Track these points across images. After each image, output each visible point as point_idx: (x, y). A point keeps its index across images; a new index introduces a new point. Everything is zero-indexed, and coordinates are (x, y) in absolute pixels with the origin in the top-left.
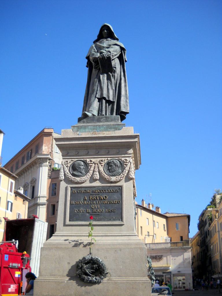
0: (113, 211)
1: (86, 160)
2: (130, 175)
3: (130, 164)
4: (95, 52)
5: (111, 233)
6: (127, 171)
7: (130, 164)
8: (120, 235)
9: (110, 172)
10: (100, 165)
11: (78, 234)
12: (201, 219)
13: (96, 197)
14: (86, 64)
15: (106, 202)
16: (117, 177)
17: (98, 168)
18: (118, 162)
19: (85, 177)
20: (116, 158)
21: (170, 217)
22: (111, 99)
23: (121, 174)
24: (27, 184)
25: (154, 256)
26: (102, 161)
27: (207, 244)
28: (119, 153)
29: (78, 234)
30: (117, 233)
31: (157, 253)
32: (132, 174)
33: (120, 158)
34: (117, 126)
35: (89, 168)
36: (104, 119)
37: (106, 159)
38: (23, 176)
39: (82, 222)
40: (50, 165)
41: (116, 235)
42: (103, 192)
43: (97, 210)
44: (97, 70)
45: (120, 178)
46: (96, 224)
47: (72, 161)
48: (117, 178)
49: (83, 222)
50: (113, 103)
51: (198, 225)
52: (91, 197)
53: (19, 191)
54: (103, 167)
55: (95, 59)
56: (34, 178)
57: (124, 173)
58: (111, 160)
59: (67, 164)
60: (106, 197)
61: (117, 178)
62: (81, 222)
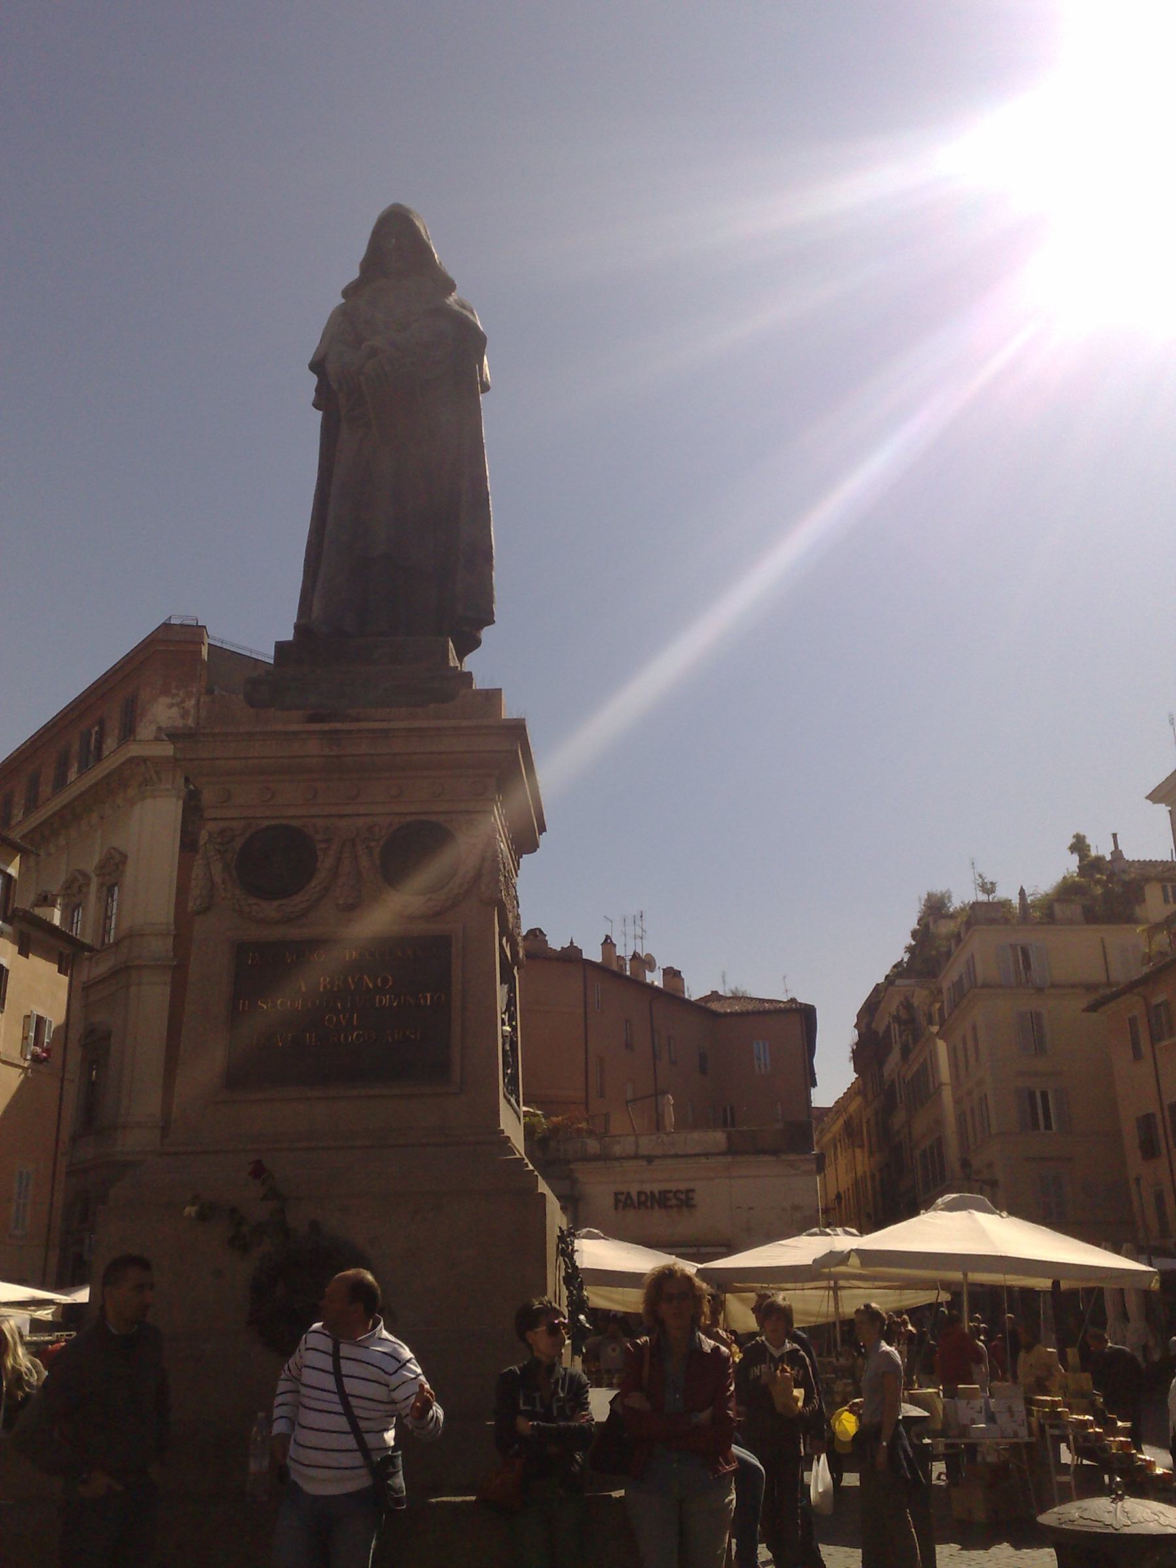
0: (413, 1037)
12: (868, 1025)
24: (80, 877)
38: (62, 841)
40: (190, 791)
43: (346, 1037)
51: (853, 1051)
53: (40, 912)
56: (114, 849)
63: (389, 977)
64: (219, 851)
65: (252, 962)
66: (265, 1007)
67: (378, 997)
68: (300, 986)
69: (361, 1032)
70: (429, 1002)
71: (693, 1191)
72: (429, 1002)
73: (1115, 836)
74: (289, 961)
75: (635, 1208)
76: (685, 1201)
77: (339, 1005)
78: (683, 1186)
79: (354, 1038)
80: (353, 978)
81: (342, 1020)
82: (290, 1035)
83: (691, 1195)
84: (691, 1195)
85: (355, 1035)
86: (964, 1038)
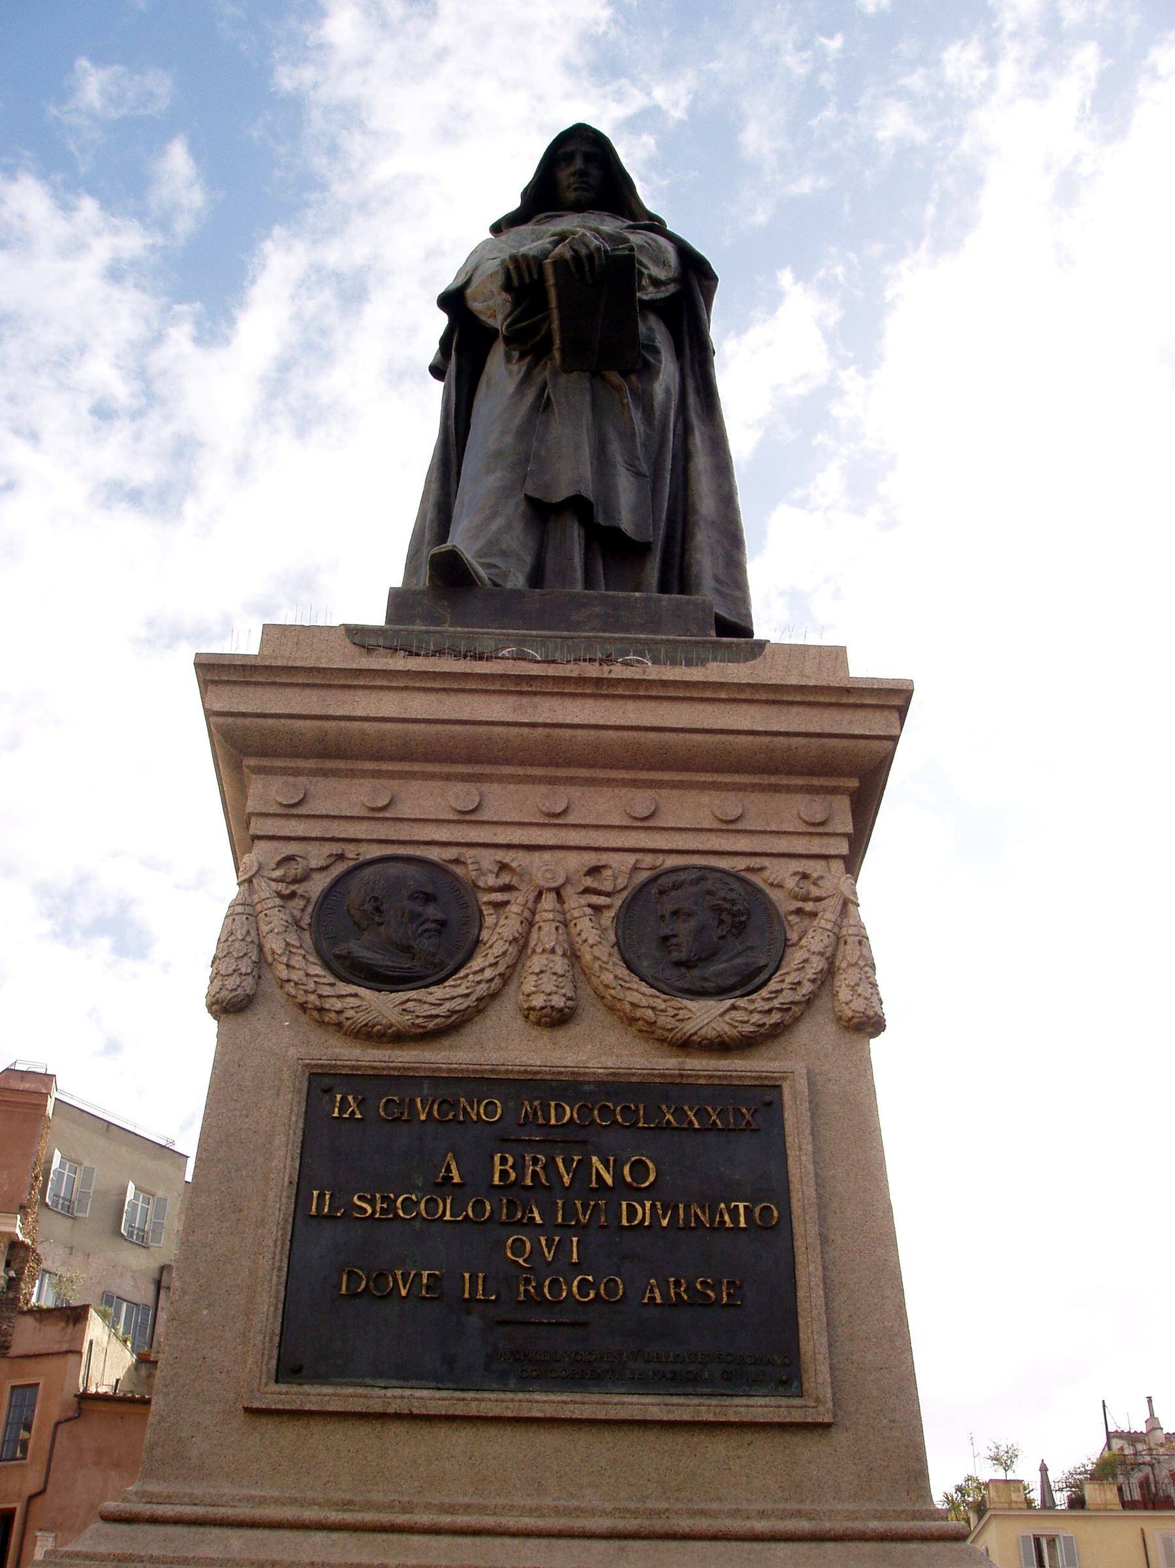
0: (712, 1294)
2: (844, 994)
5: (703, 1513)
6: (818, 964)
8: (804, 1525)
9: (678, 964)
10: (575, 903)
11: (369, 1506)
13: (554, 1159)
14: (430, 350)
15: (644, 1212)
16: (741, 1002)
17: (566, 924)
18: (736, 885)
22: (626, 521)
23: (773, 985)
26: (594, 871)
28: (739, 826)
29: (369, 1506)
30: (762, 1514)
33: (755, 862)
35: (490, 920)
36: (597, 609)
37: (631, 859)
39: (407, 1392)
40: (11, 1279)
41: (760, 1526)
42: (615, 1122)
43: (555, 1282)
44: (522, 356)
45: (770, 1011)
46: (549, 1411)
48: (734, 1007)
49: (418, 1393)
50: (641, 550)
52: (504, 1161)
54: (608, 917)
55: (528, 267)
58: (675, 870)
59: (296, 881)
60: (639, 1168)
62: (398, 1392)
63: (651, 1165)
64: (279, 895)
65: (339, 1113)
66: (370, 1210)
67: (624, 1204)
68: (449, 1169)
69: (590, 1278)
70: (742, 1219)
72: (742, 1219)
73: (1150, 1399)
74: (423, 1117)
77: (536, 1215)
79: (575, 1289)
80: (567, 1162)
81: (546, 1250)
82: (425, 1273)
85: (575, 1283)
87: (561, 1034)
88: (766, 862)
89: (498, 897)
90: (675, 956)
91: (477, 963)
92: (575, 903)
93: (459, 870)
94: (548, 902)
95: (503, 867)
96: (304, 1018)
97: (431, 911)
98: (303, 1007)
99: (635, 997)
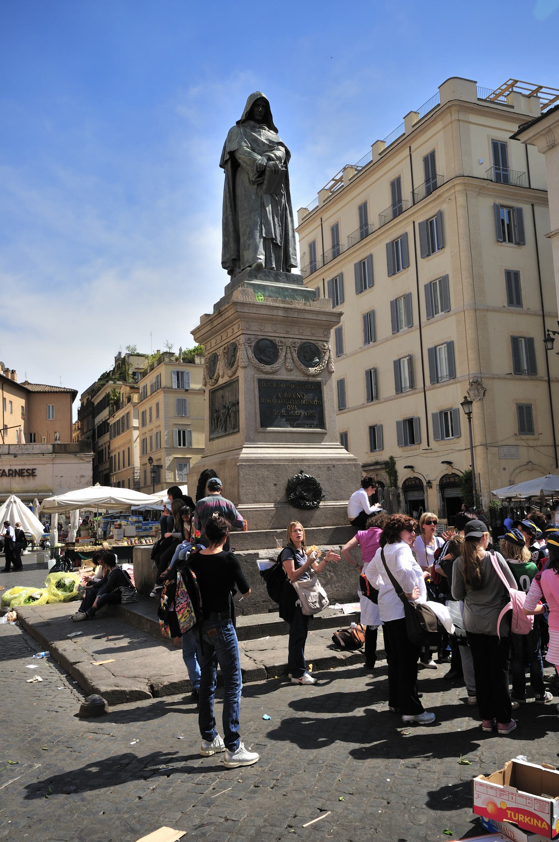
1: (275, 340)
3: (330, 353)
4: (248, 147)
6: (326, 362)
7: (330, 353)
9: (307, 361)
19: (277, 366)
20: (312, 342)
21: (35, 392)
25: (18, 470)
27: (101, 449)
31: (25, 464)
32: (333, 367)
33: (317, 342)
34: (305, 293)
35: (280, 352)
47: (257, 338)
50: (280, 247)
54: (297, 353)
57: (324, 364)
58: (305, 343)
59: (250, 343)
61: (316, 370)
71: (35, 469)
75: (7, 476)
76: (32, 473)
78: (31, 467)
83: (34, 471)
84: (34, 471)
86: (151, 409)
87: (291, 373)
88: (318, 342)
89: (281, 347)
90: (306, 359)
91: (280, 360)
92: (292, 349)
93: (274, 341)
94: (288, 348)
95: (281, 341)
96: (255, 369)
97: (271, 350)
98: (255, 367)
99: (302, 367)
